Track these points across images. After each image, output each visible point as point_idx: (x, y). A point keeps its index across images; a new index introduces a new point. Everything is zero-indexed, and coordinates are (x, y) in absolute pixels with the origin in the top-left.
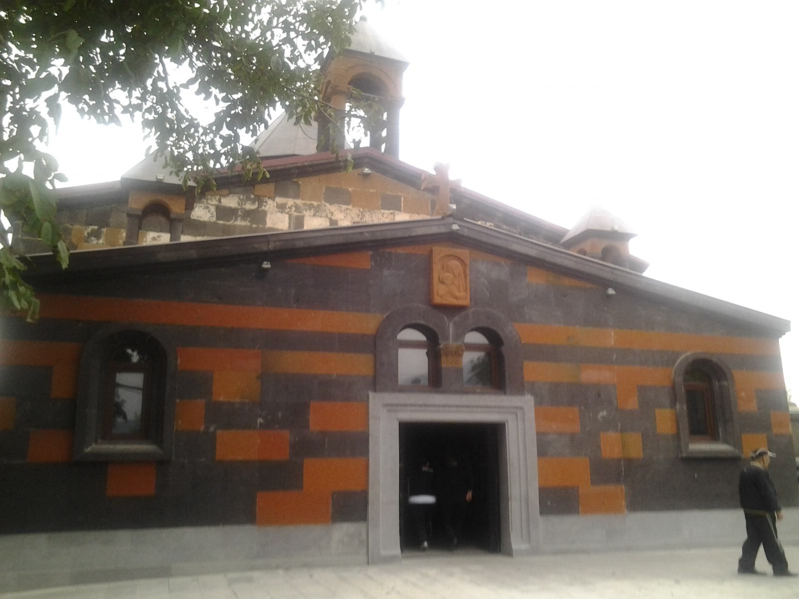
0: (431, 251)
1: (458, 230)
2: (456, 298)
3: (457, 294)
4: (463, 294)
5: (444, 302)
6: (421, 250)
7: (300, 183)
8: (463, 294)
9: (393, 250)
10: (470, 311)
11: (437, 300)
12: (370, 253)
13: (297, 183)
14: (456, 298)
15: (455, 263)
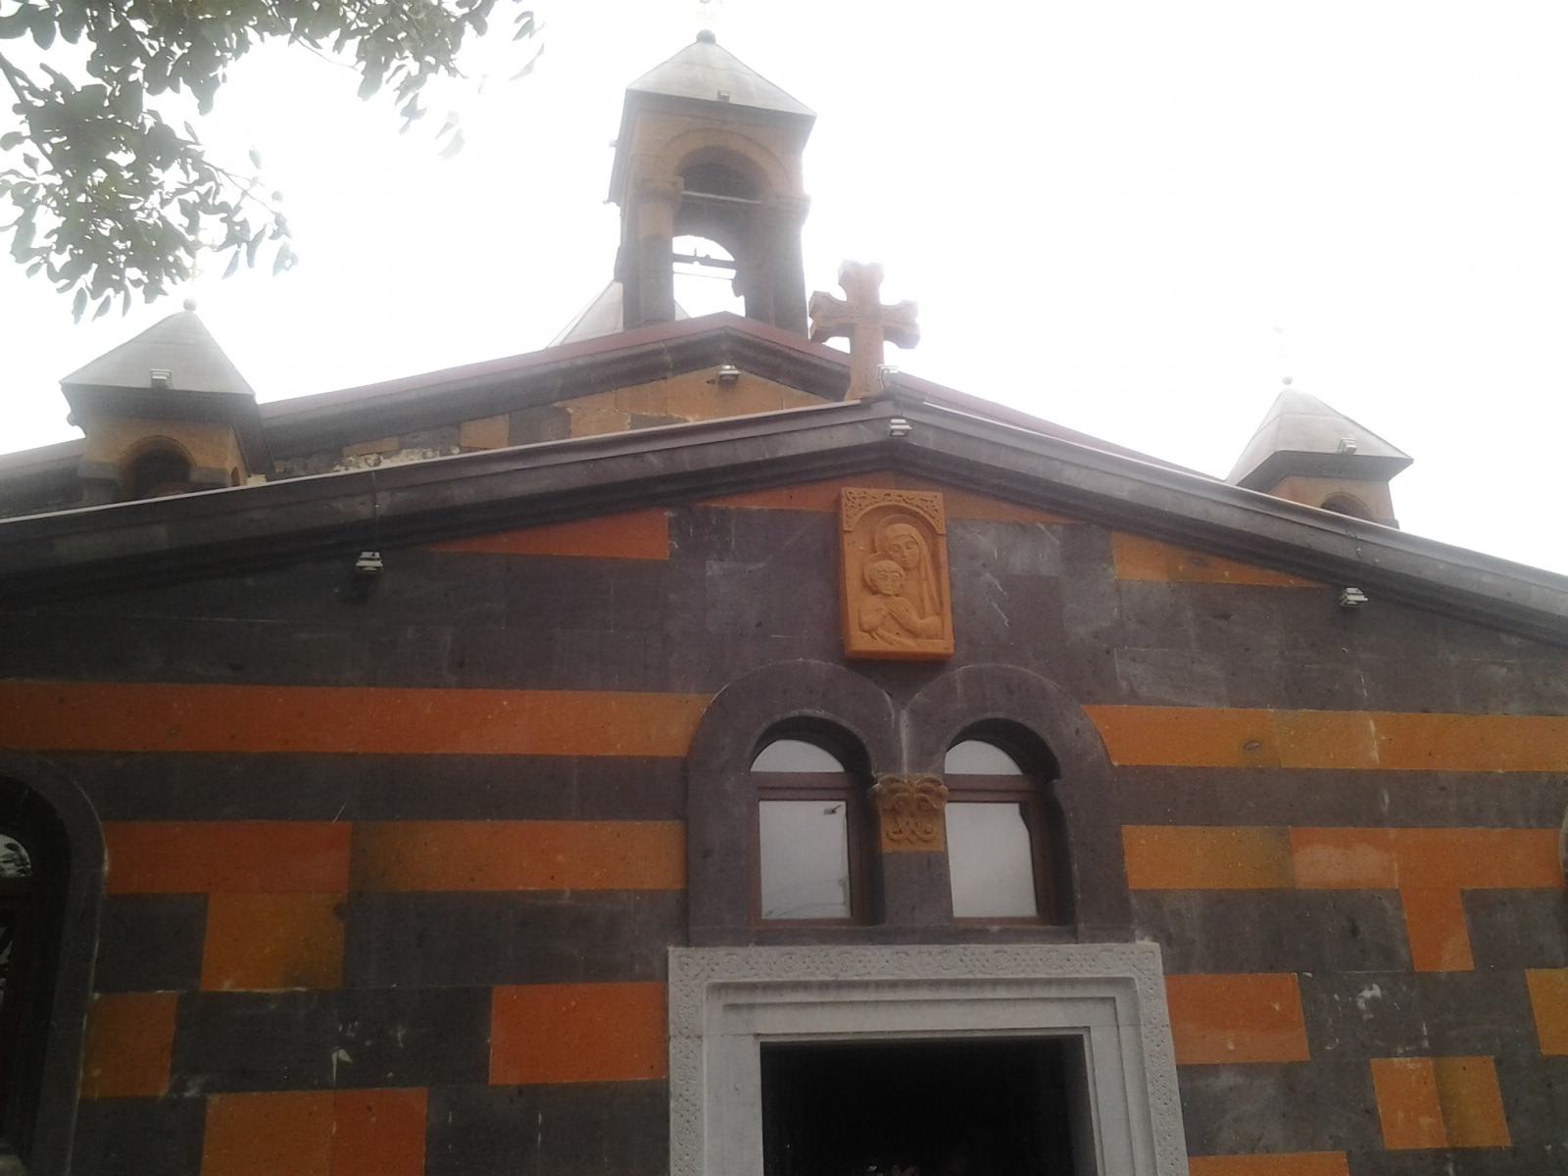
0: (837, 502)
1: (907, 432)
2: (914, 634)
3: (917, 621)
4: (931, 620)
5: (879, 646)
6: (811, 500)
7: (570, 411)
8: (931, 620)
9: (732, 505)
10: (958, 673)
11: (861, 643)
12: (668, 514)
13: (561, 411)
14: (914, 634)
15: (905, 530)
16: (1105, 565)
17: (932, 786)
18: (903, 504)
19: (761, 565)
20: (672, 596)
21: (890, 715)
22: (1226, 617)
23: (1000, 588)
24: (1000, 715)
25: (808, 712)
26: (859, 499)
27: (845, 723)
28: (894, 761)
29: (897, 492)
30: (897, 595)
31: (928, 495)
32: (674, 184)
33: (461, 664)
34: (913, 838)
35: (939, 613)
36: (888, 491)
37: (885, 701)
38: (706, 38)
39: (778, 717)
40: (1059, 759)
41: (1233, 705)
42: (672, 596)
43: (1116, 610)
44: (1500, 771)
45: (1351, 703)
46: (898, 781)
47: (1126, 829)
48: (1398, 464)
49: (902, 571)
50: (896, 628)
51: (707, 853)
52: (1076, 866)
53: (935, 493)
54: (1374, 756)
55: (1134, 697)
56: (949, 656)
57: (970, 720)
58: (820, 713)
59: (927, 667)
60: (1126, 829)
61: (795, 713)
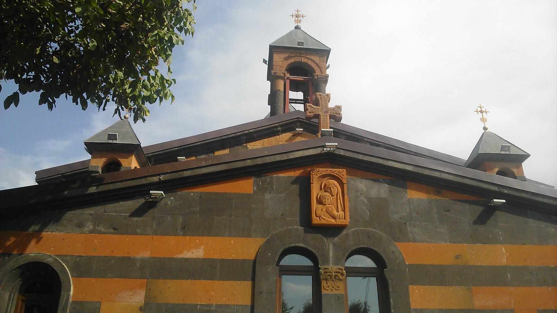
2: (334, 218)
7: (248, 146)
8: (341, 213)
11: (316, 220)
14: (334, 218)
16: (404, 194)
17: (340, 270)
18: (332, 173)
19: (283, 195)
20: (253, 206)
21: (326, 246)
22: (449, 211)
23: (366, 202)
24: (366, 246)
25: (298, 245)
26: (317, 172)
27: (310, 248)
28: (326, 261)
29: (331, 169)
30: (329, 204)
31: (341, 170)
32: (284, 74)
33: (184, 228)
34: (333, 289)
35: (344, 211)
36: (327, 169)
37: (324, 241)
38: (297, 28)
39: (287, 246)
40: (387, 262)
41: (451, 242)
42: (253, 206)
43: (408, 209)
44: (552, 266)
45: (495, 241)
46: (327, 269)
47: (411, 287)
48: (526, 156)
49: (331, 196)
50: (329, 216)
51: (261, 293)
52: (392, 300)
53: (343, 170)
54: (504, 261)
55: (415, 240)
56: (347, 225)
57: (354, 248)
58: (302, 245)
59: (340, 228)
60: (411, 287)
61: (293, 245)
